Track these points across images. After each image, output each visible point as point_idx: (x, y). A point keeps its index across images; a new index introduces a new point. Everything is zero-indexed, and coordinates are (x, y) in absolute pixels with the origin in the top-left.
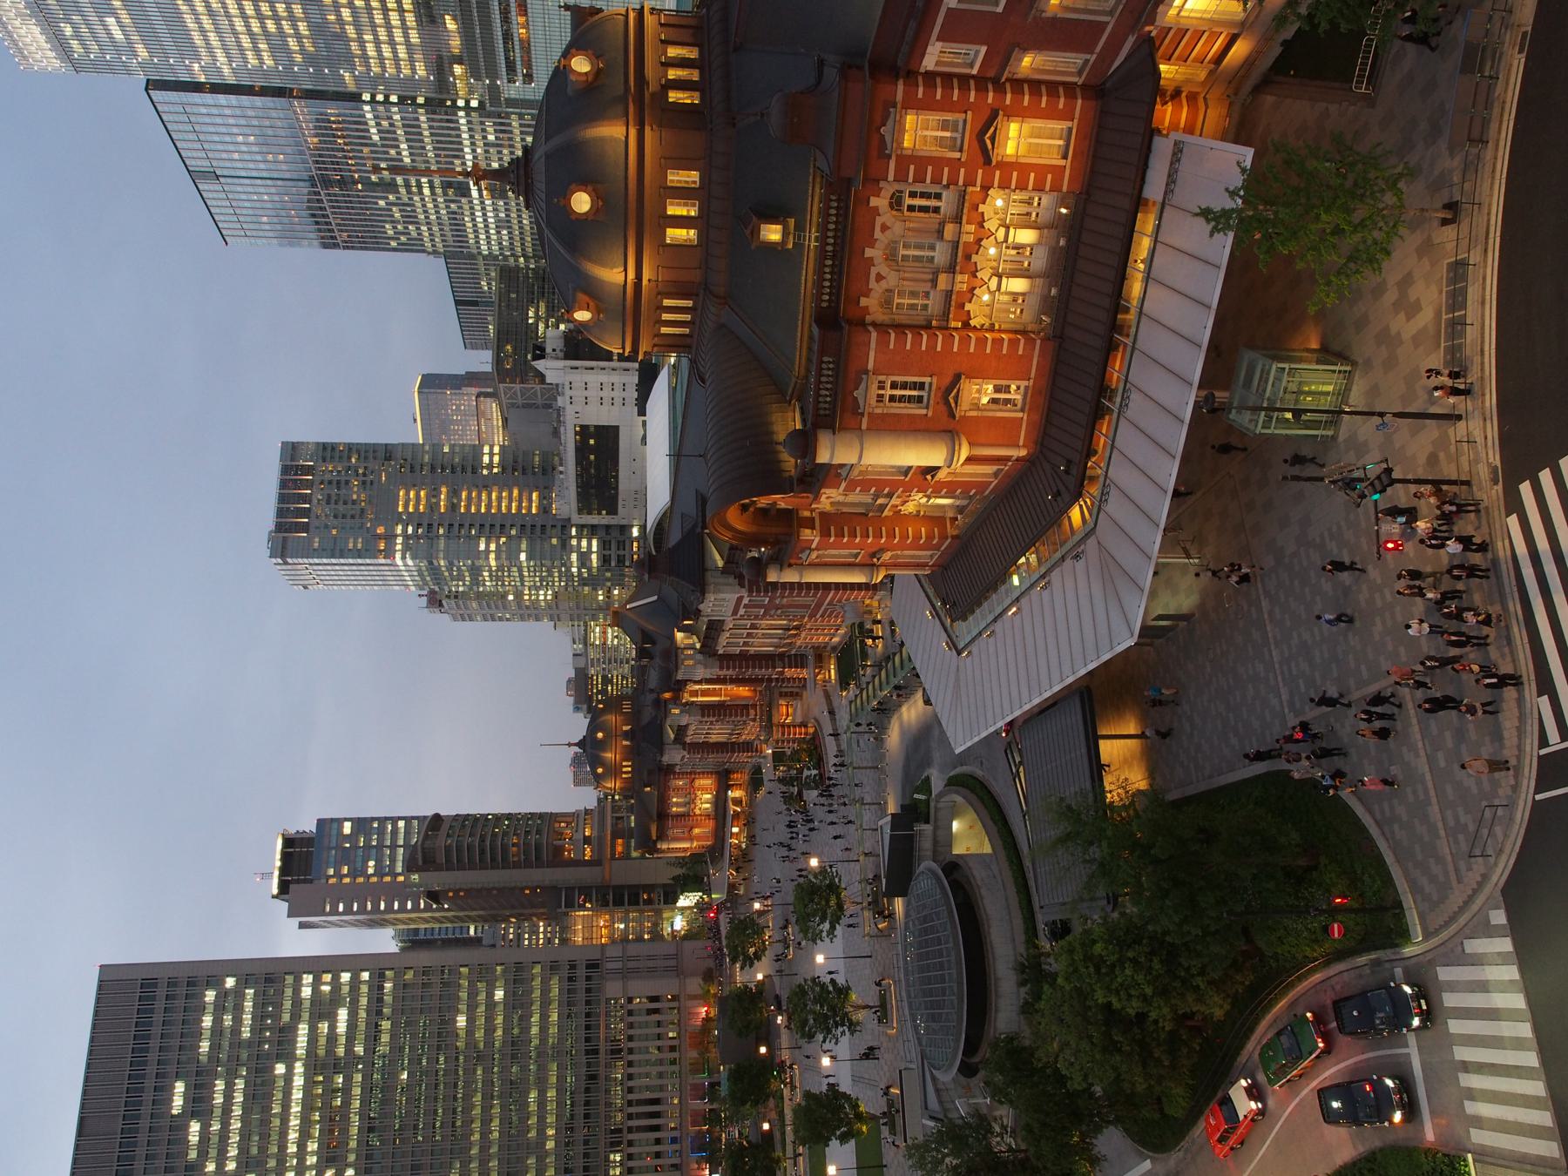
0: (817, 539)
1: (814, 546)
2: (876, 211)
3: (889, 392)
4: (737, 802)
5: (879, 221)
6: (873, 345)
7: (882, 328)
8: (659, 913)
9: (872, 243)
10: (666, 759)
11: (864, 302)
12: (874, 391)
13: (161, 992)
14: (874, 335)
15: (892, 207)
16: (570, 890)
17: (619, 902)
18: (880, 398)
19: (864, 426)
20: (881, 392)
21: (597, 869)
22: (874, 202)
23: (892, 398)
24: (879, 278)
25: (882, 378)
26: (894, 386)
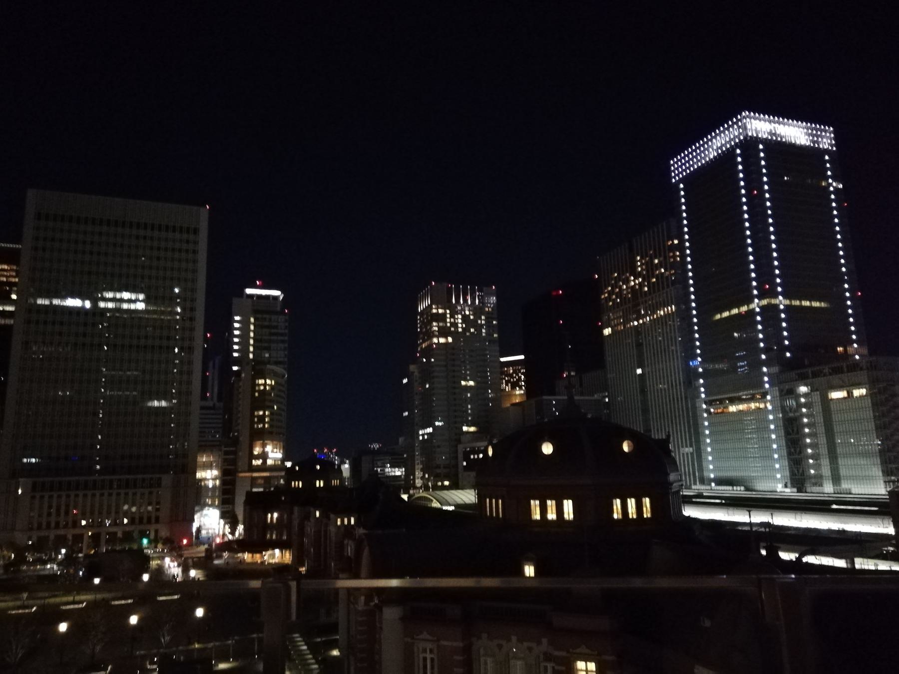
0: (360, 608)
1: (356, 606)
2: (539, 643)
3: (429, 656)
4: (273, 556)
5: (534, 645)
6: (455, 644)
7: (467, 650)
8: (217, 507)
9: (520, 641)
10: (296, 509)
11: (484, 636)
12: (429, 646)
13: (192, 237)
14: (461, 645)
15: (545, 654)
16: (235, 453)
17: (223, 483)
18: (425, 651)
19: (406, 639)
20: (428, 652)
21: (246, 468)
22: (545, 641)
23: (425, 659)
24: (500, 647)
25: (435, 651)
26: (432, 660)
